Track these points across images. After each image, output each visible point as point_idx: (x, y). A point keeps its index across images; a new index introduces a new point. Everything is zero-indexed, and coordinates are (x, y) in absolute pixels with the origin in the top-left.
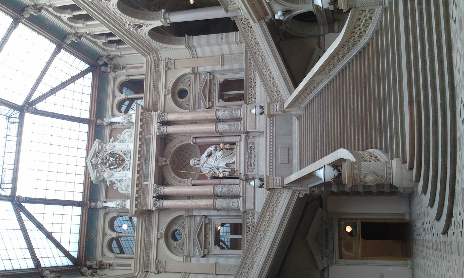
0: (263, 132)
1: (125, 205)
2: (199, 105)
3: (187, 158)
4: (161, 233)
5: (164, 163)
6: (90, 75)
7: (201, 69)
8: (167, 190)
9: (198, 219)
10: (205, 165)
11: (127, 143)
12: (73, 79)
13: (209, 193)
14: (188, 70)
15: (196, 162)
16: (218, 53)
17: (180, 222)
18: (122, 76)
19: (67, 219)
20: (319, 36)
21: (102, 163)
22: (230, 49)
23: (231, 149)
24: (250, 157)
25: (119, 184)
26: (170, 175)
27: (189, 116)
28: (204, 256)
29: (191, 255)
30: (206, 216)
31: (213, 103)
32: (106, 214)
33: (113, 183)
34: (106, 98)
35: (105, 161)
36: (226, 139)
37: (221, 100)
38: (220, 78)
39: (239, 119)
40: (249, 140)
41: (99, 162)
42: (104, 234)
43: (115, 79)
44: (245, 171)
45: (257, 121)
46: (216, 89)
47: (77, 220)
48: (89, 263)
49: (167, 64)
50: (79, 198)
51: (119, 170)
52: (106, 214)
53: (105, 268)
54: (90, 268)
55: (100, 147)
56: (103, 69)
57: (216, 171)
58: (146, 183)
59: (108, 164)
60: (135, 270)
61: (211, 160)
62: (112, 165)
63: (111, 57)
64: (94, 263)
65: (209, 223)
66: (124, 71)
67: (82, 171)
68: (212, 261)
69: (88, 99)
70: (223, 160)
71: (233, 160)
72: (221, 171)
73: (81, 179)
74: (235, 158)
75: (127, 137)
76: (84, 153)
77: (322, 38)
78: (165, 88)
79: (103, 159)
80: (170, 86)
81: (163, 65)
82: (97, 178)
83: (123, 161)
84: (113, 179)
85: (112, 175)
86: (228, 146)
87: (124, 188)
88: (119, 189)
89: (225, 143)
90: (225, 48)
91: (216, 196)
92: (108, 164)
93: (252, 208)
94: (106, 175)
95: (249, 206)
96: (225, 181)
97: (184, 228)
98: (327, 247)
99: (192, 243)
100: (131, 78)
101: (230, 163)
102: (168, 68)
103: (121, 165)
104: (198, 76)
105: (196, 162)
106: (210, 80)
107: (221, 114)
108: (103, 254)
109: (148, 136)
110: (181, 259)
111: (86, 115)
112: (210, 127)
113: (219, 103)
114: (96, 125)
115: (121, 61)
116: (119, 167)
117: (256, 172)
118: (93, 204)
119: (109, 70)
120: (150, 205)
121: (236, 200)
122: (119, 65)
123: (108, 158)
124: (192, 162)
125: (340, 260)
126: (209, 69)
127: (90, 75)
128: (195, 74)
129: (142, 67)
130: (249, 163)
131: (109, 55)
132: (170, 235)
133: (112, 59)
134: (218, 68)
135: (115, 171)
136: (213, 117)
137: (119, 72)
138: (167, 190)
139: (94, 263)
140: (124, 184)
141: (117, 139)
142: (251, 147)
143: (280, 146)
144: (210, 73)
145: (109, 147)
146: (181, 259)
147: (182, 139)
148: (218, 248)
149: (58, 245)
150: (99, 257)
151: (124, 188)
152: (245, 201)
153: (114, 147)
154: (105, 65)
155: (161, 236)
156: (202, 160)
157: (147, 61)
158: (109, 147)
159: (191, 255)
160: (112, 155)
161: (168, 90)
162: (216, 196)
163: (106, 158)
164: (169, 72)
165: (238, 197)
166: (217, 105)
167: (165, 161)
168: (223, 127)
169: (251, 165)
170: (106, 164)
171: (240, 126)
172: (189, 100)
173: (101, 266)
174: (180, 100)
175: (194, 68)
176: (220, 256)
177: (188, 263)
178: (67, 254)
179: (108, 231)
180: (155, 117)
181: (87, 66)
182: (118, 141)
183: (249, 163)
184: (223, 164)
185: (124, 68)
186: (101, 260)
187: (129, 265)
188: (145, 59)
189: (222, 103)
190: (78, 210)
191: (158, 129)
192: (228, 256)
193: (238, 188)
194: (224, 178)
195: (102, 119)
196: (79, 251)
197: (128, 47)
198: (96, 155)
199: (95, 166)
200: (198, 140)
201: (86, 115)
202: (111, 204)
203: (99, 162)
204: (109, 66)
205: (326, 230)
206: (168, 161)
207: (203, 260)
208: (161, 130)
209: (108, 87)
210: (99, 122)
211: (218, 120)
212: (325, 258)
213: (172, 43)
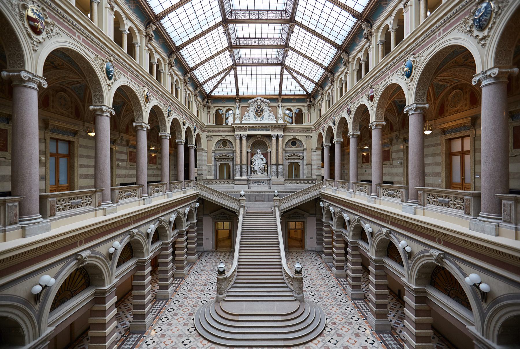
0: (270, 188)
1: (237, 120)
2: (288, 153)
3: (261, 147)
4: (225, 137)
5: (258, 137)
6: (305, 93)
7: (305, 154)
8: (244, 141)
9: (231, 155)
10: (257, 157)
11: (268, 117)
12: (302, 86)
13: (243, 162)
14: (305, 147)
15: (259, 153)
16: (313, 162)
17: (231, 146)
18: (305, 110)
19: (229, 89)
20: (315, 214)
21: (258, 105)
22: (314, 169)
23: (264, 169)
24: (259, 182)
25: (248, 115)
26: (252, 141)
27: (280, 150)
28: (215, 159)
29: (216, 152)
30: (233, 159)
31: (288, 160)
32: (234, 107)
33: (248, 111)
34: (293, 102)
35: (259, 106)
36: (269, 168)
37: (289, 164)
38: (300, 163)
39: (277, 176)
40: (267, 182)
41: (258, 104)
42: (224, 107)
43: (304, 106)
44: (253, 180)
45: (276, 185)
46: (296, 161)
47: (230, 93)
48: (209, 101)
49: (309, 136)
50: (241, 93)
51: (255, 114)
52: (234, 107)
53: (208, 109)
54: (207, 102)
55: (266, 103)
56: (309, 100)
57: (254, 164)
58: (247, 130)
59: (257, 108)
60: (207, 126)
61: (260, 160)
62: (257, 111)
63: (314, 105)
64: (210, 104)
65: (230, 160)
66: (307, 112)
67: (254, 93)
68: (213, 163)
69: (292, 93)
70: (258, 168)
71: (258, 173)
72: (254, 166)
73: (250, 93)
74: (260, 174)
75: (272, 117)
76: (263, 93)
77: (315, 215)
78: (296, 135)
79: (260, 105)
80: (297, 137)
81: (308, 133)
82: (250, 103)
83: (259, 116)
84: (250, 111)
85: (252, 111)
86: (266, 169)
87: (245, 118)
88: (245, 115)
89: (267, 167)
90: (314, 167)
91: (241, 165)
92: (257, 108)
93: (236, 184)
94: (252, 108)
95: (236, 182)
96: (249, 168)
97: (228, 148)
98: (219, 217)
99: (221, 152)
100: (304, 115)
101: (257, 172)
102: (307, 136)
103: (257, 115)
104: (302, 152)
105: (259, 153)
106: (300, 158)
107: (280, 167)
108: (214, 107)
109: (271, 130)
110: (213, 148)
111: (283, 93)
112: (274, 162)
113: (288, 163)
114: (278, 99)
115: (312, 109)
116: (256, 114)
117: (252, 185)
118: (238, 101)
119: (308, 103)
120: (237, 133)
121: (239, 175)
122: (310, 108)
123: (261, 108)
124: (259, 151)
125: (214, 222)
126: (305, 158)
127: (305, 93)
128: (303, 150)
129: (308, 121)
130: (256, 182)
131: (315, 104)
132: (225, 141)
133: (313, 105)
134: (305, 163)
135: (254, 113)
136: (279, 163)
137: (307, 108)
138: (244, 141)
139: (210, 104)
140: (247, 118)
141: (270, 112)
142: (264, 183)
143: (264, 196)
144: (303, 158)
145: (266, 108)
146: (213, 148)
147: (270, 145)
148: (219, 164)
149: (216, 87)
150: (213, 106)
151: (245, 118)
152: (239, 180)
153: (266, 111)
154: (311, 102)
155: (224, 137)
156: (260, 155)
157: (311, 125)
158: (266, 108)
159: (216, 152)
160: (262, 111)
161: (295, 137)
162: (241, 165)
163: (260, 107)
164: (305, 137)
165: (241, 176)
166: (287, 162)
167: (259, 138)
168: (274, 168)
169: (255, 183)
170: (258, 107)
171: (274, 177)
172: (290, 147)
173: (209, 108)
174: (290, 143)
175: (306, 150)
176: (215, 166)
177: (212, 152)
178: (212, 91)
179: (226, 108)
180: (281, 133)
181: (310, 93)
182: (269, 113)
183: (256, 182)
184: (256, 169)
185: (309, 111)
186: (212, 106)
187: (210, 122)
188: (312, 124)
189: (287, 164)
190: (235, 93)
191: (275, 135)
192: (215, 170)
193: (244, 177)
194: (251, 168)
195: (282, 102)
196: (214, 96)
197: (318, 117)
198: (262, 101)
199: (256, 101)
200: (269, 154)
201: (283, 93)
202: (238, 112)
203: (258, 104)
204: (310, 103)
205: (226, 217)
206: (260, 139)
207: (213, 158)
208: (274, 136)
209: (300, 103)
210: (280, 100)
211: (277, 165)
212: (214, 216)
213: (318, 141)
